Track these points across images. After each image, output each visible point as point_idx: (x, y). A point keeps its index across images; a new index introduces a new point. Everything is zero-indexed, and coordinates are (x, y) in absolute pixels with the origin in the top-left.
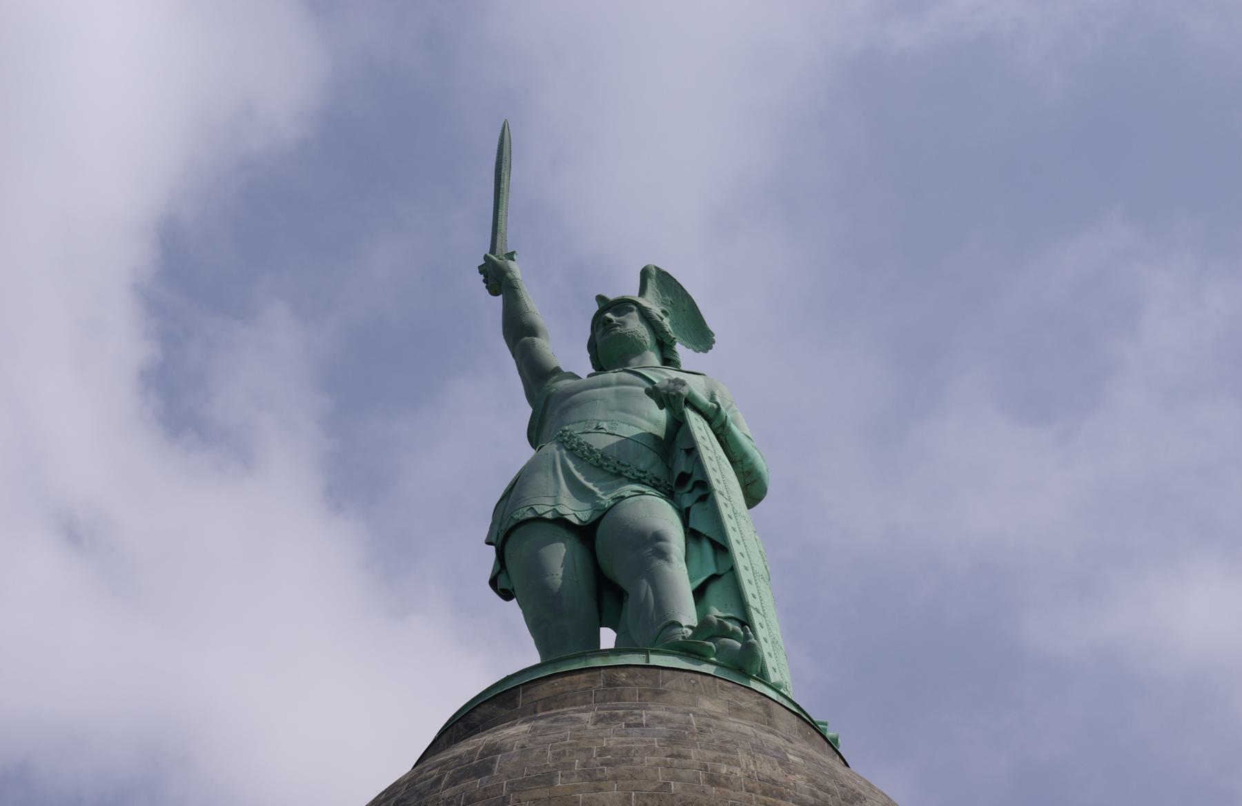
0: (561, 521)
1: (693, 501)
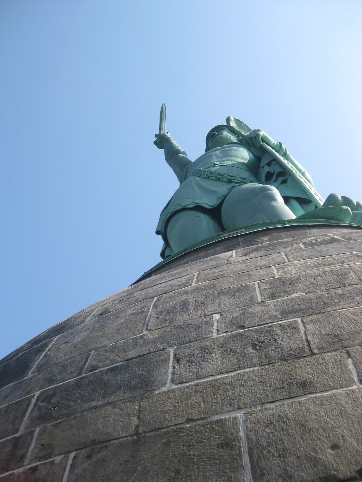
0: (198, 208)
1: (279, 184)
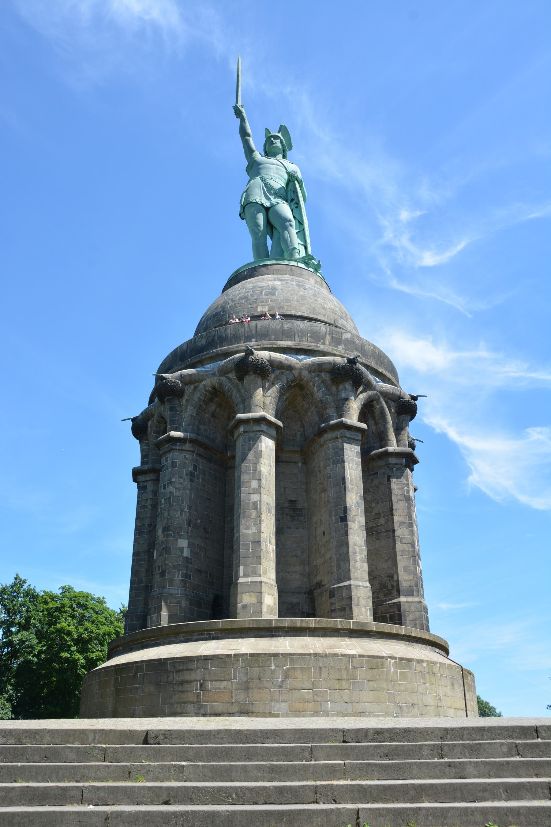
0: (262, 205)
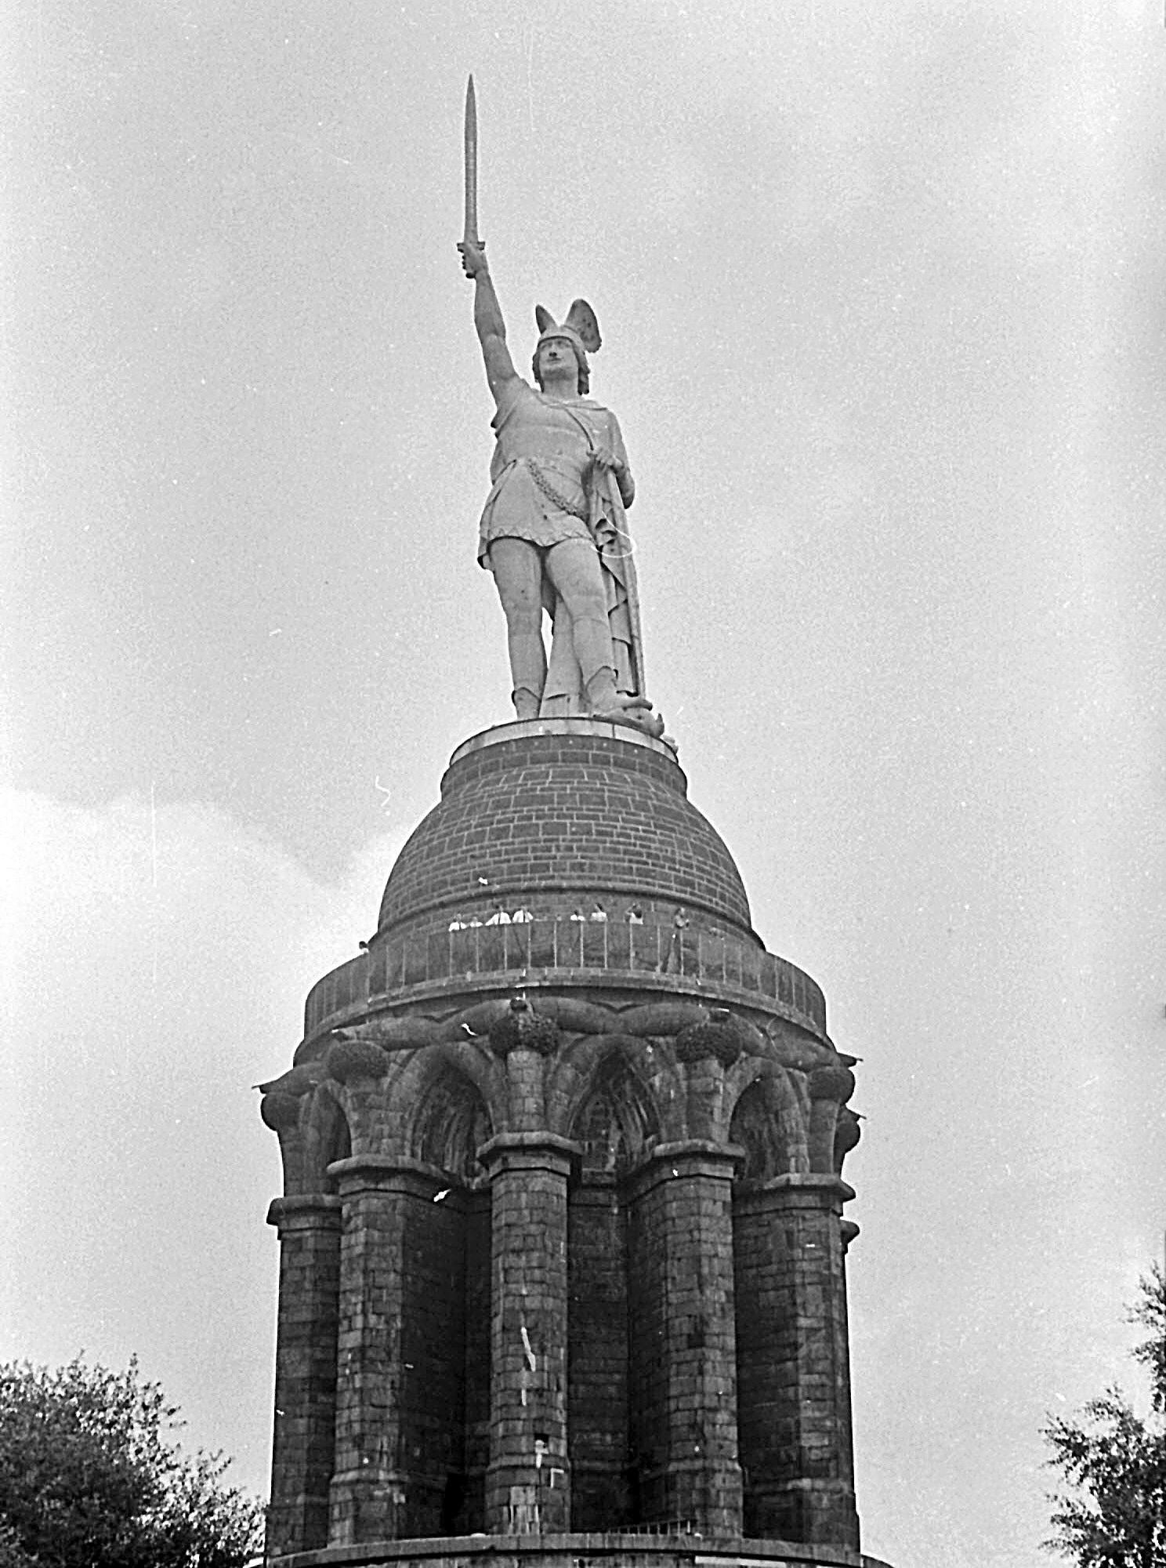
0: (532, 543)
